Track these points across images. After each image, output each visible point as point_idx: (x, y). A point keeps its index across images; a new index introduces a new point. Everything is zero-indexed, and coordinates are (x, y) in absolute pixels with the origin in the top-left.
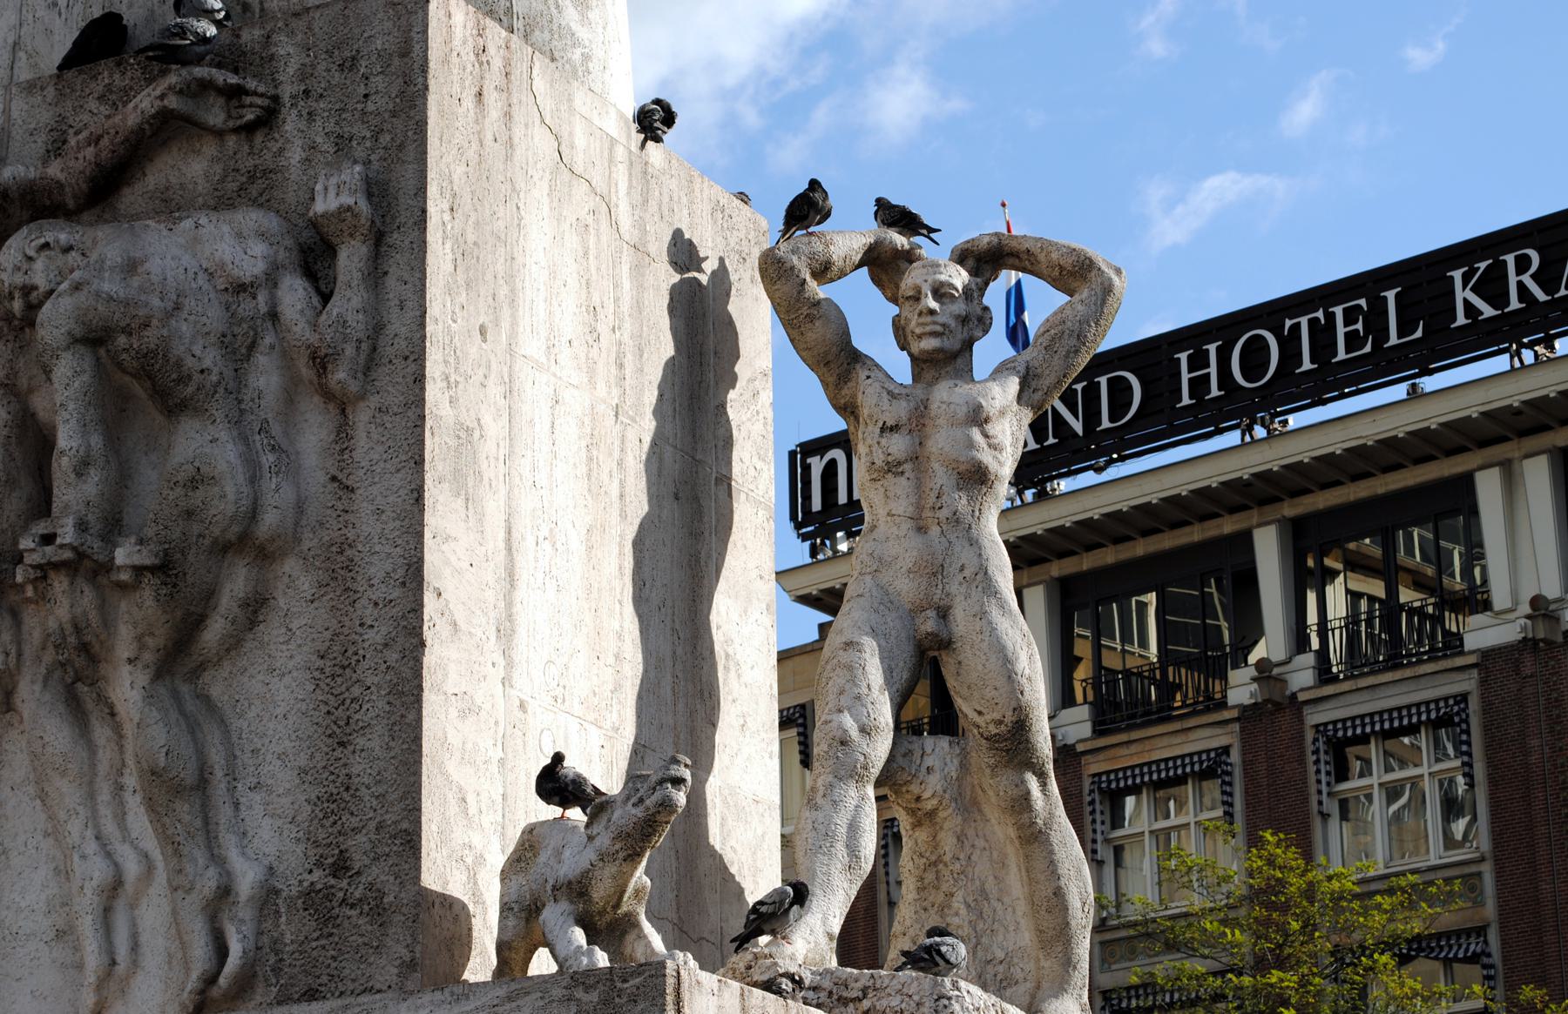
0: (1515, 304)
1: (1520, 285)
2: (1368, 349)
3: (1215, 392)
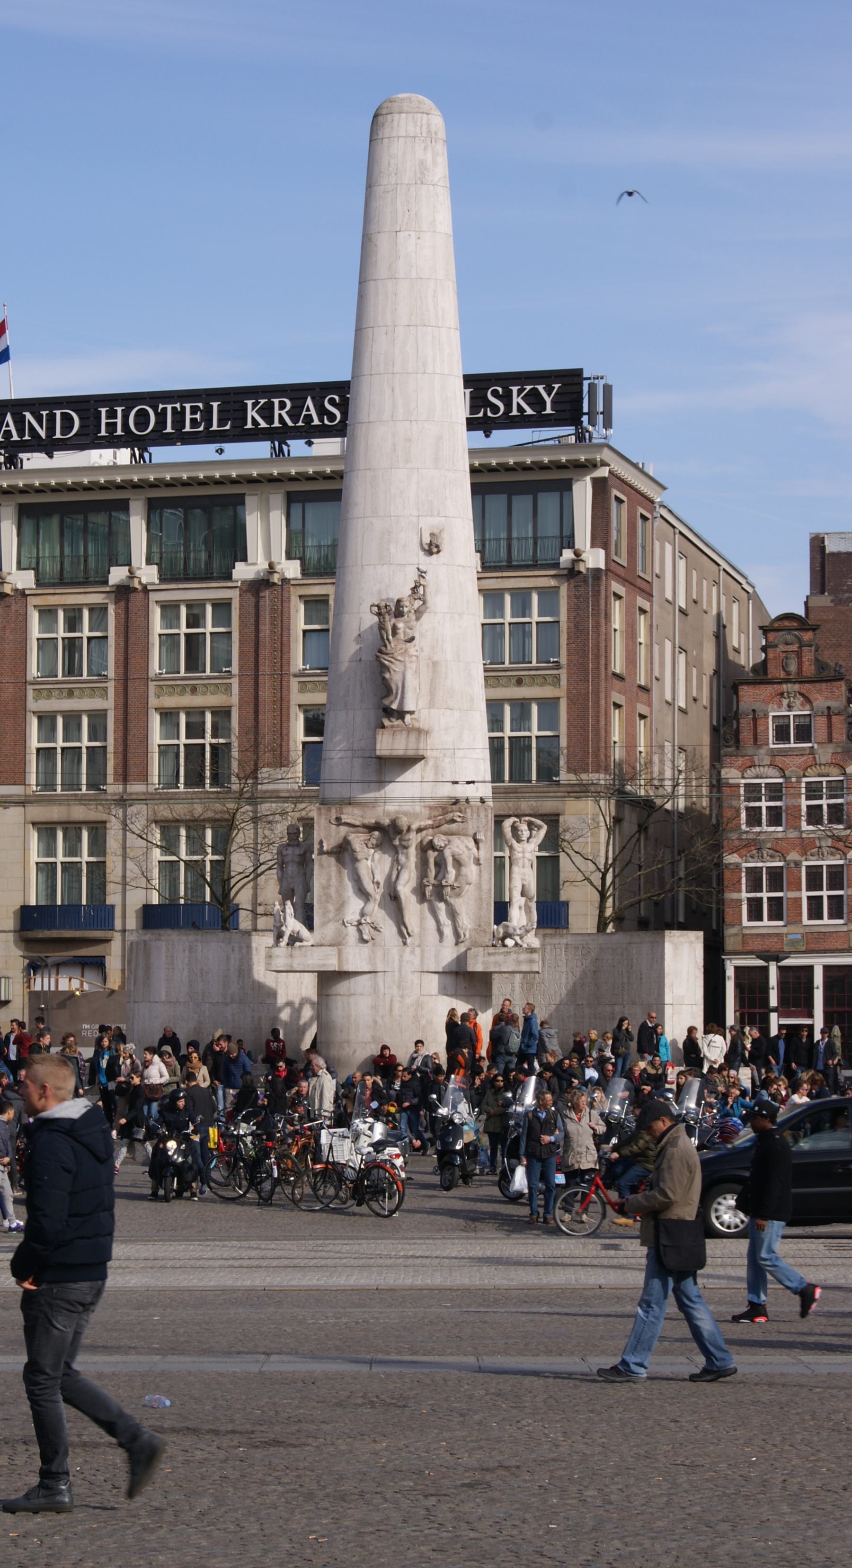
0: (276, 424)
1: (280, 416)
2: (201, 429)
3: (119, 432)
